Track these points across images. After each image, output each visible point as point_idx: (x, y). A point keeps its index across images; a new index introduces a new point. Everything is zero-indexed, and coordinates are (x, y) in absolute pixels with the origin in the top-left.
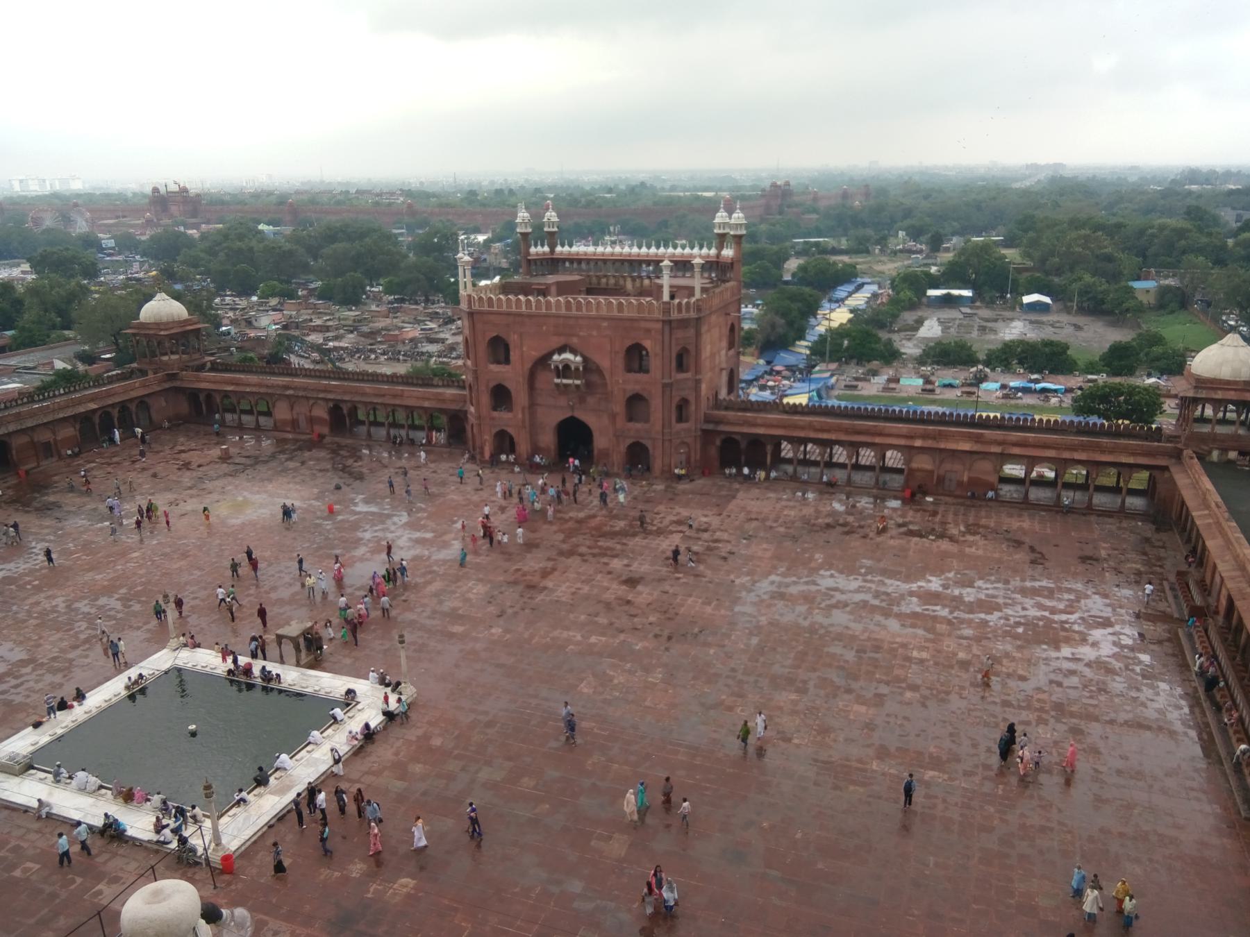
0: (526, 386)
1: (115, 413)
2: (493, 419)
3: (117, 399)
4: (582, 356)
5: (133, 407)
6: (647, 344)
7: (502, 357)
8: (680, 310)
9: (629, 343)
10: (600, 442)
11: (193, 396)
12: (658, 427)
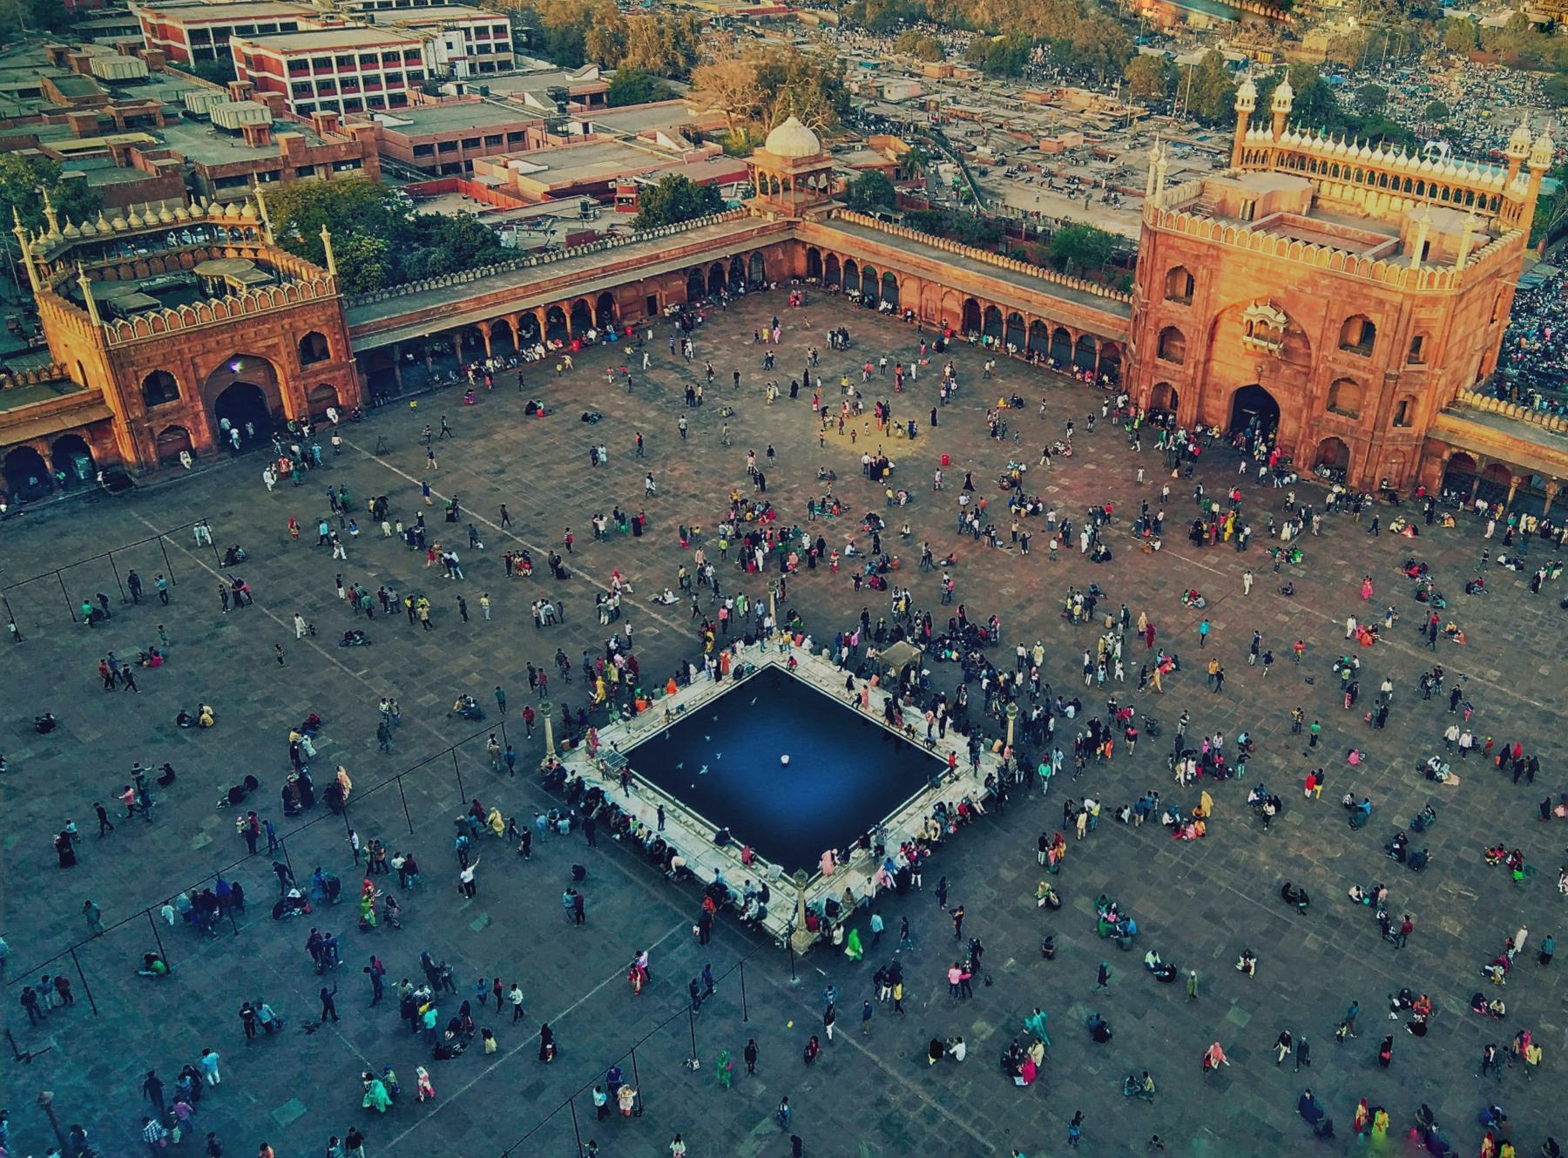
0: (1206, 337)
1: (727, 266)
2: (1156, 367)
3: (731, 251)
4: (1285, 314)
5: (746, 260)
6: (1376, 318)
7: (1182, 290)
8: (1430, 283)
9: (1351, 311)
10: (1288, 426)
11: (813, 253)
12: (1368, 426)
